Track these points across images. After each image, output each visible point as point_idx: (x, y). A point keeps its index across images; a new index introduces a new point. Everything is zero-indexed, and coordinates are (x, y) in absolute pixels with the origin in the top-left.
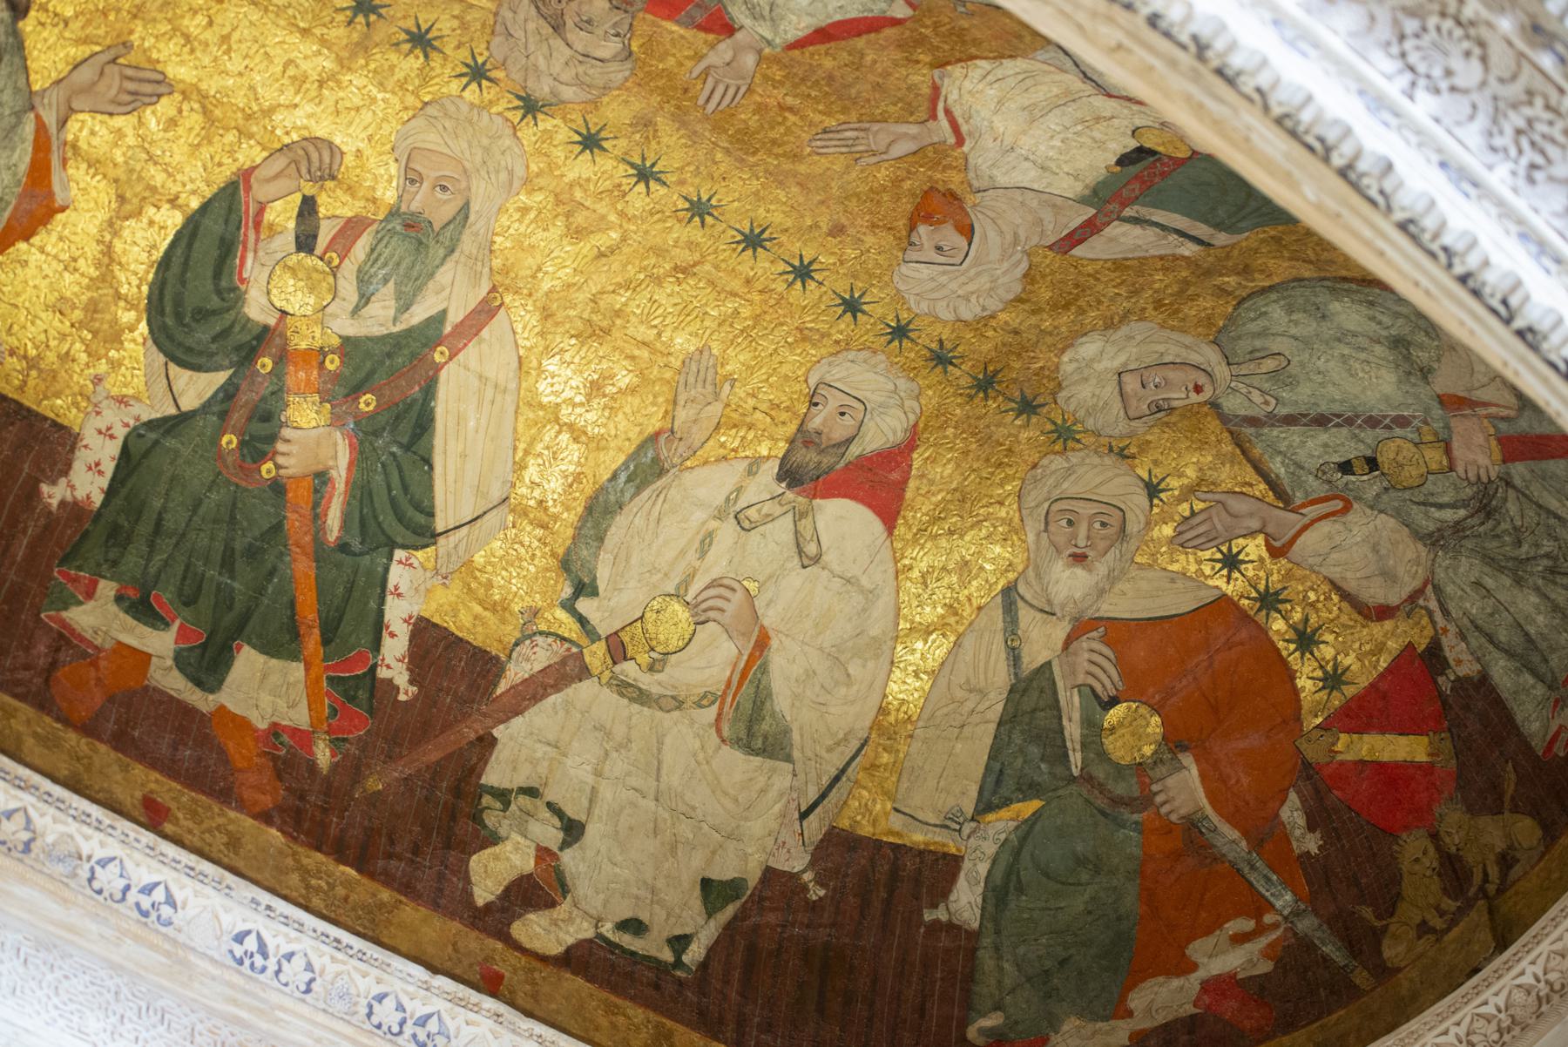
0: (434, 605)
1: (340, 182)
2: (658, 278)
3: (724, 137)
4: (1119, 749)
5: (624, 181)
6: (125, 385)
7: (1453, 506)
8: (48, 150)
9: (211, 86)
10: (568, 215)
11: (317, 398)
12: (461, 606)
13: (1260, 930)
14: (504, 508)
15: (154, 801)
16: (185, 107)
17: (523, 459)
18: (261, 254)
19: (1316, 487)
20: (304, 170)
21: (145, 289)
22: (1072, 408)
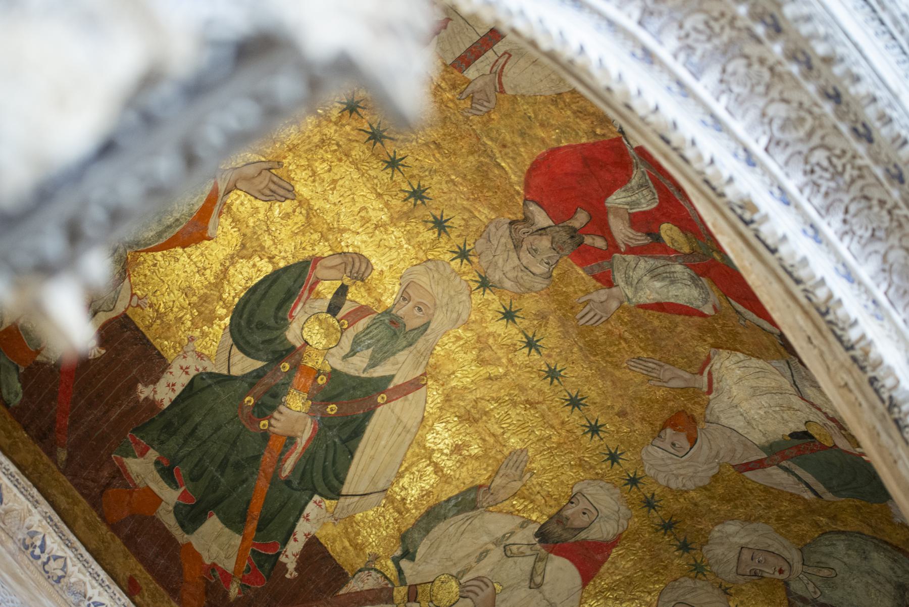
0: (324, 533)
1: (365, 284)
2: (515, 402)
3: (583, 340)
5: (519, 343)
6: (205, 348)
8: (215, 203)
9: (317, 204)
10: (481, 350)
11: (306, 396)
12: (338, 539)
14: (383, 495)
15: (135, 581)
16: (298, 210)
17: (403, 472)
18: (307, 306)
20: (348, 270)
21: (237, 300)
22: (709, 556)
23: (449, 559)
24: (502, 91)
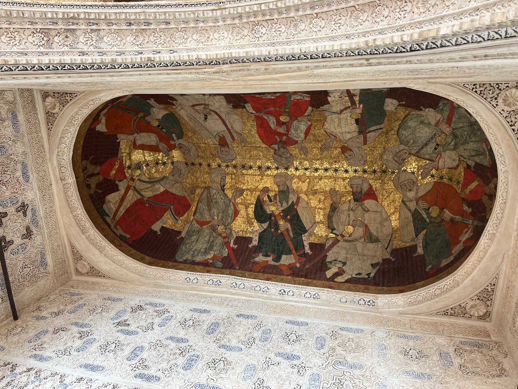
4: (434, 214)
7: (452, 141)
24: (241, 134)
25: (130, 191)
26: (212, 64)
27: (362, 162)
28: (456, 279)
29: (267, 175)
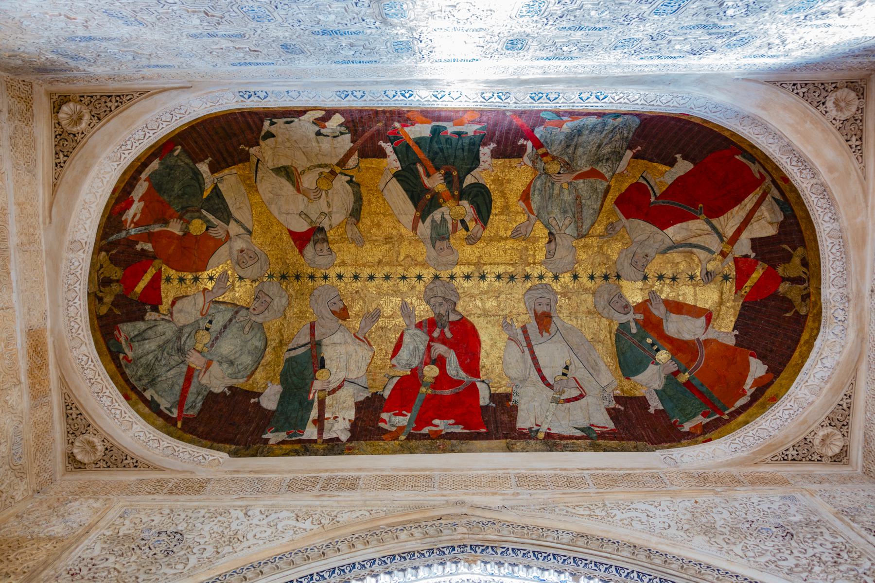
13: (132, 222)
19: (211, 311)
23: (337, 193)
25: (731, 234)
26: (484, 548)
27: (316, 293)
28: (115, 164)
29: (469, 264)
